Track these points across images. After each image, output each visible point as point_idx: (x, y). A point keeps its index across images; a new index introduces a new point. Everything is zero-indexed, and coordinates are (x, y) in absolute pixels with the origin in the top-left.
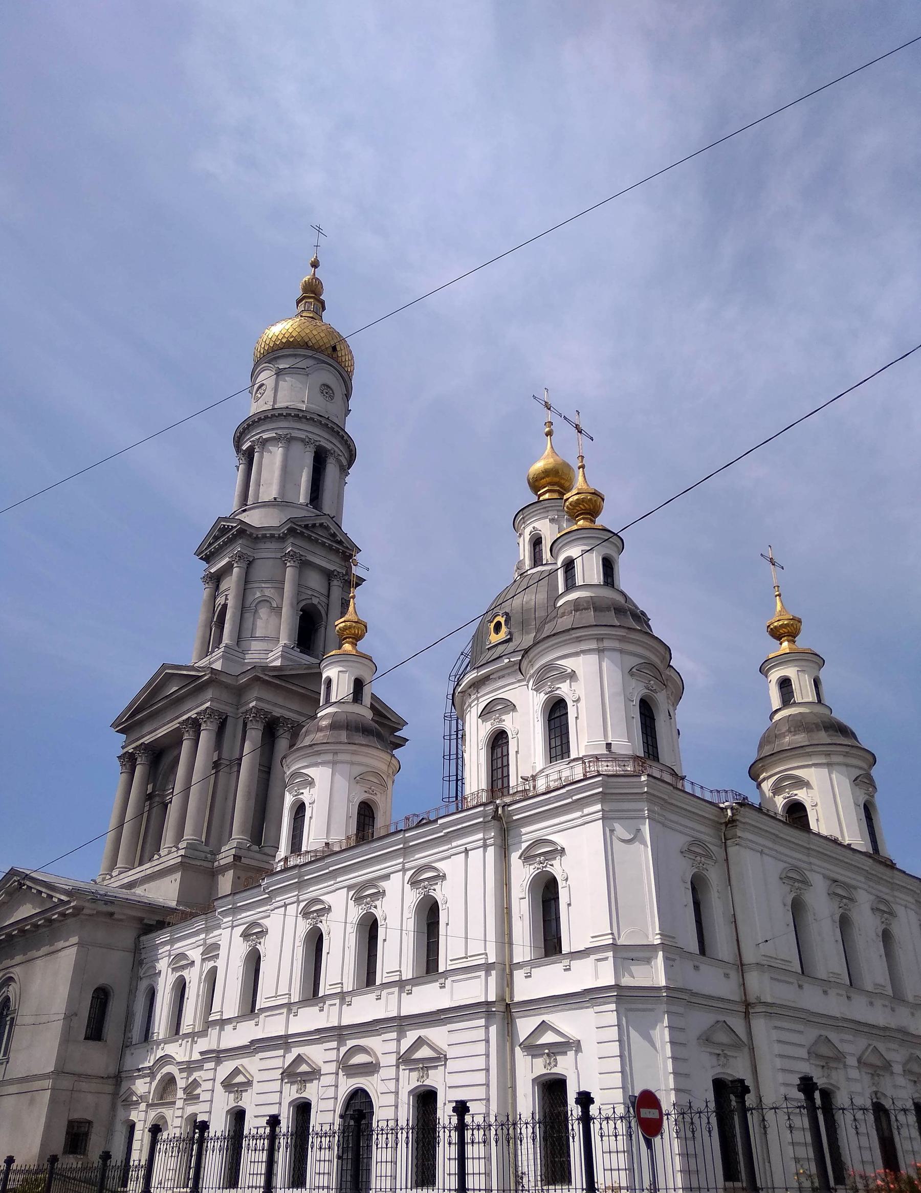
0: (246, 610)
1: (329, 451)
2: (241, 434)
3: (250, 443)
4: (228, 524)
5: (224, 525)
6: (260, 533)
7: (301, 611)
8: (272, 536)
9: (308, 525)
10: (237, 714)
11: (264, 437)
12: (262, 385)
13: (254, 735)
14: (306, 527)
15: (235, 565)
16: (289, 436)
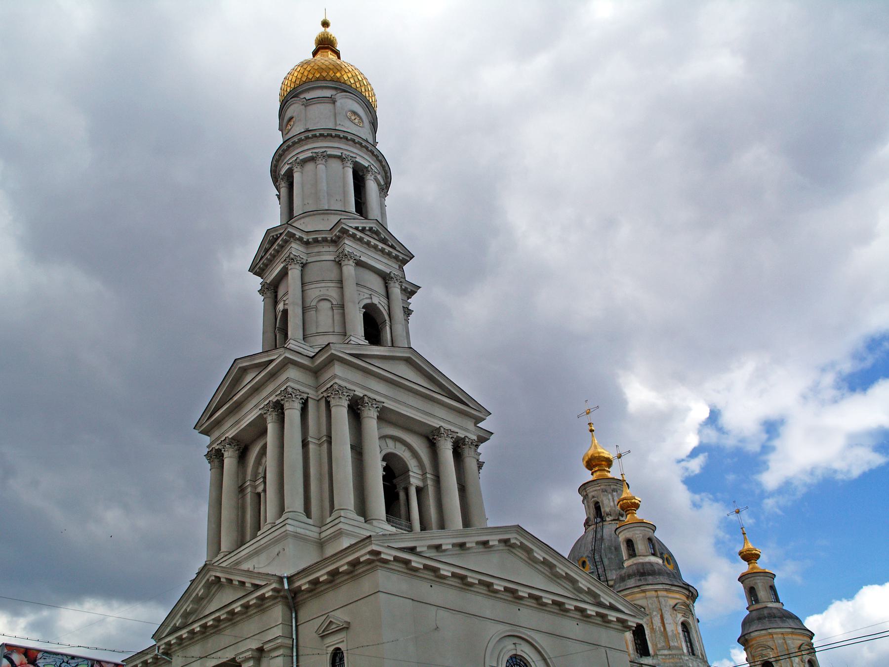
0: (306, 310)
1: (367, 168)
2: (278, 161)
3: (288, 166)
4: (277, 233)
5: (273, 236)
6: (311, 237)
7: (363, 308)
8: (325, 240)
9: (358, 227)
10: (318, 396)
11: (301, 158)
12: (291, 119)
13: (341, 413)
14: (357, 228)
15: (289, 268)
16: (325, 154)
